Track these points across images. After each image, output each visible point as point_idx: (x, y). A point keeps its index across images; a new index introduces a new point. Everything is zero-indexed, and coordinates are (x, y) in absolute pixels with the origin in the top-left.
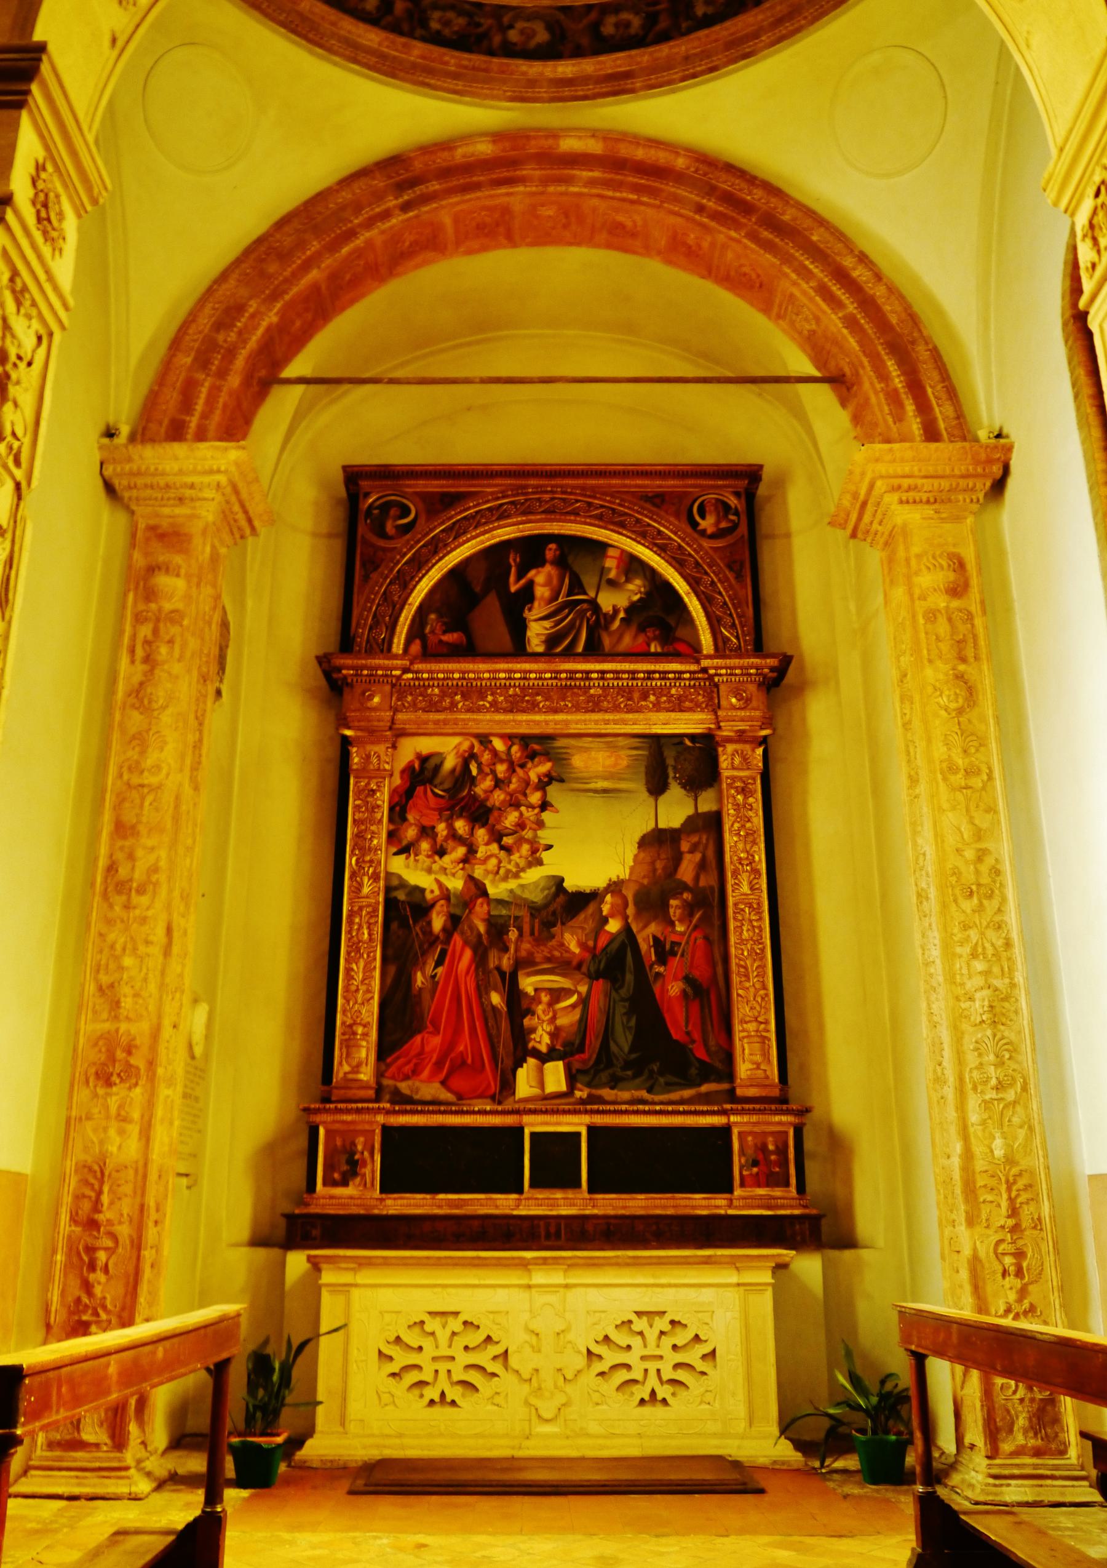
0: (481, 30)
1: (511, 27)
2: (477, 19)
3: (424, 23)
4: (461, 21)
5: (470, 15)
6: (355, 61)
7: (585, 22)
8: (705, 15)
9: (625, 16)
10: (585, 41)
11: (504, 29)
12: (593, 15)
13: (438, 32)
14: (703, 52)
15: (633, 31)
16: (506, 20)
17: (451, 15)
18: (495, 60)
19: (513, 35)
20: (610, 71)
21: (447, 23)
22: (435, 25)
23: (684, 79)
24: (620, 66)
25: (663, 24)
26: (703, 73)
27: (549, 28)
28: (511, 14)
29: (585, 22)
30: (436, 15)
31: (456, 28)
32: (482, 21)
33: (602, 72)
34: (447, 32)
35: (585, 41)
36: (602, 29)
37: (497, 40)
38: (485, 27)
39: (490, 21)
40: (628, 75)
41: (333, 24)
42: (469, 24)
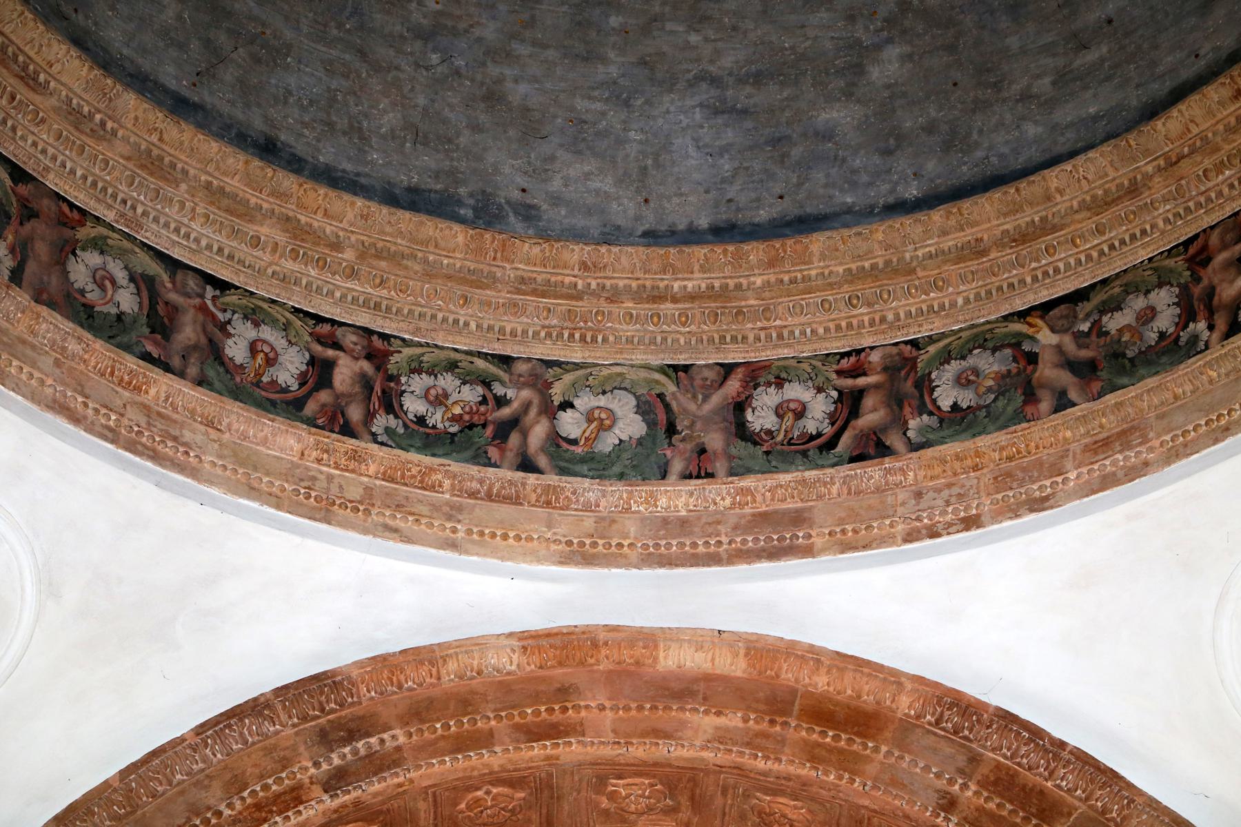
0: (506, 412)
1: (567, 405)
2: (499, 390)
3: (391, 404)
4: (471, 394)
5: (487, 384)
6: (252, 491)
7: (716, 399)
8: (955, 407)
9: (795, 391)
10: (715, 440)
11: (551, 410)
12: (733, 385)
13: (421, 420)
14: (949, 486)
15: (812, 428)
16: (557, 393)
17: (447, 382)
18: (532, 478)
19: (570, 424)
20: (764, 508)
21: (440, 400)
22: (414, 406)
23: (910, 538)
24: (783, 500)
25: (872, 415)
26: (949, 528)
27: (643, 409)
28: (568, 378)
29: (716, 399)
30: (418, 383)
31: (457, 410)
32: (510, 393)
33: (747, 510)
34: (437, 418)
35: (715, 440)
36: (749, 416)
37: (538, 433)
38: (515, 405)
39: (526, 393)
40: (798, 519)
41: (210, 424)
42: (484, 401)
